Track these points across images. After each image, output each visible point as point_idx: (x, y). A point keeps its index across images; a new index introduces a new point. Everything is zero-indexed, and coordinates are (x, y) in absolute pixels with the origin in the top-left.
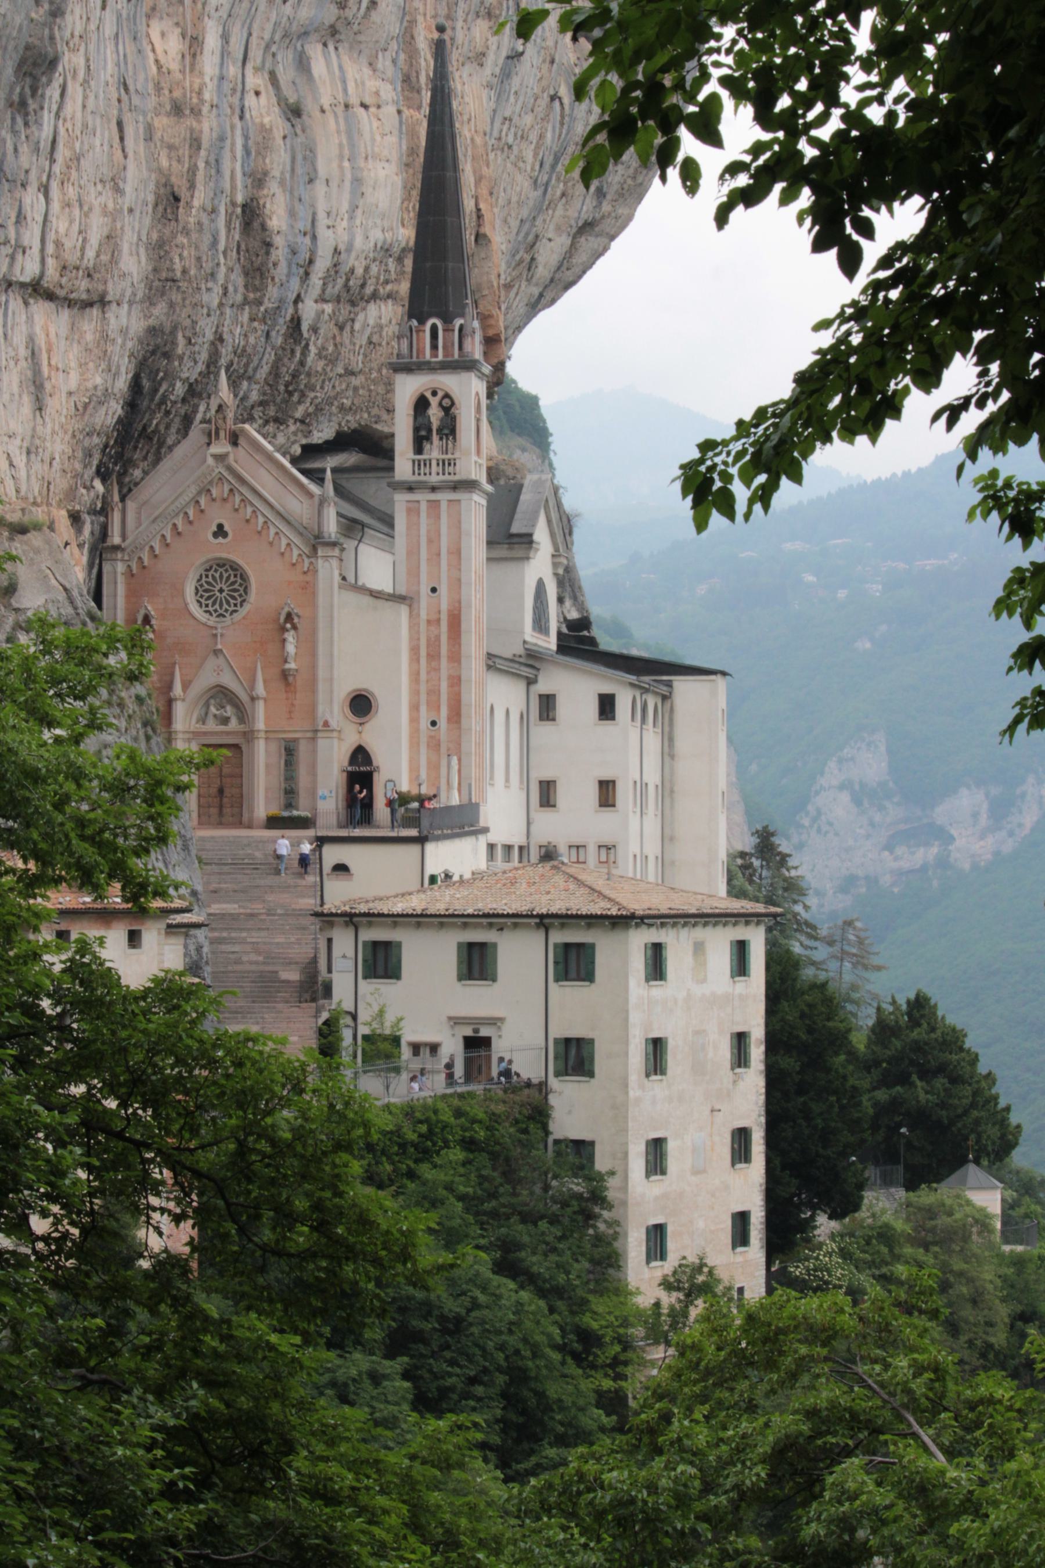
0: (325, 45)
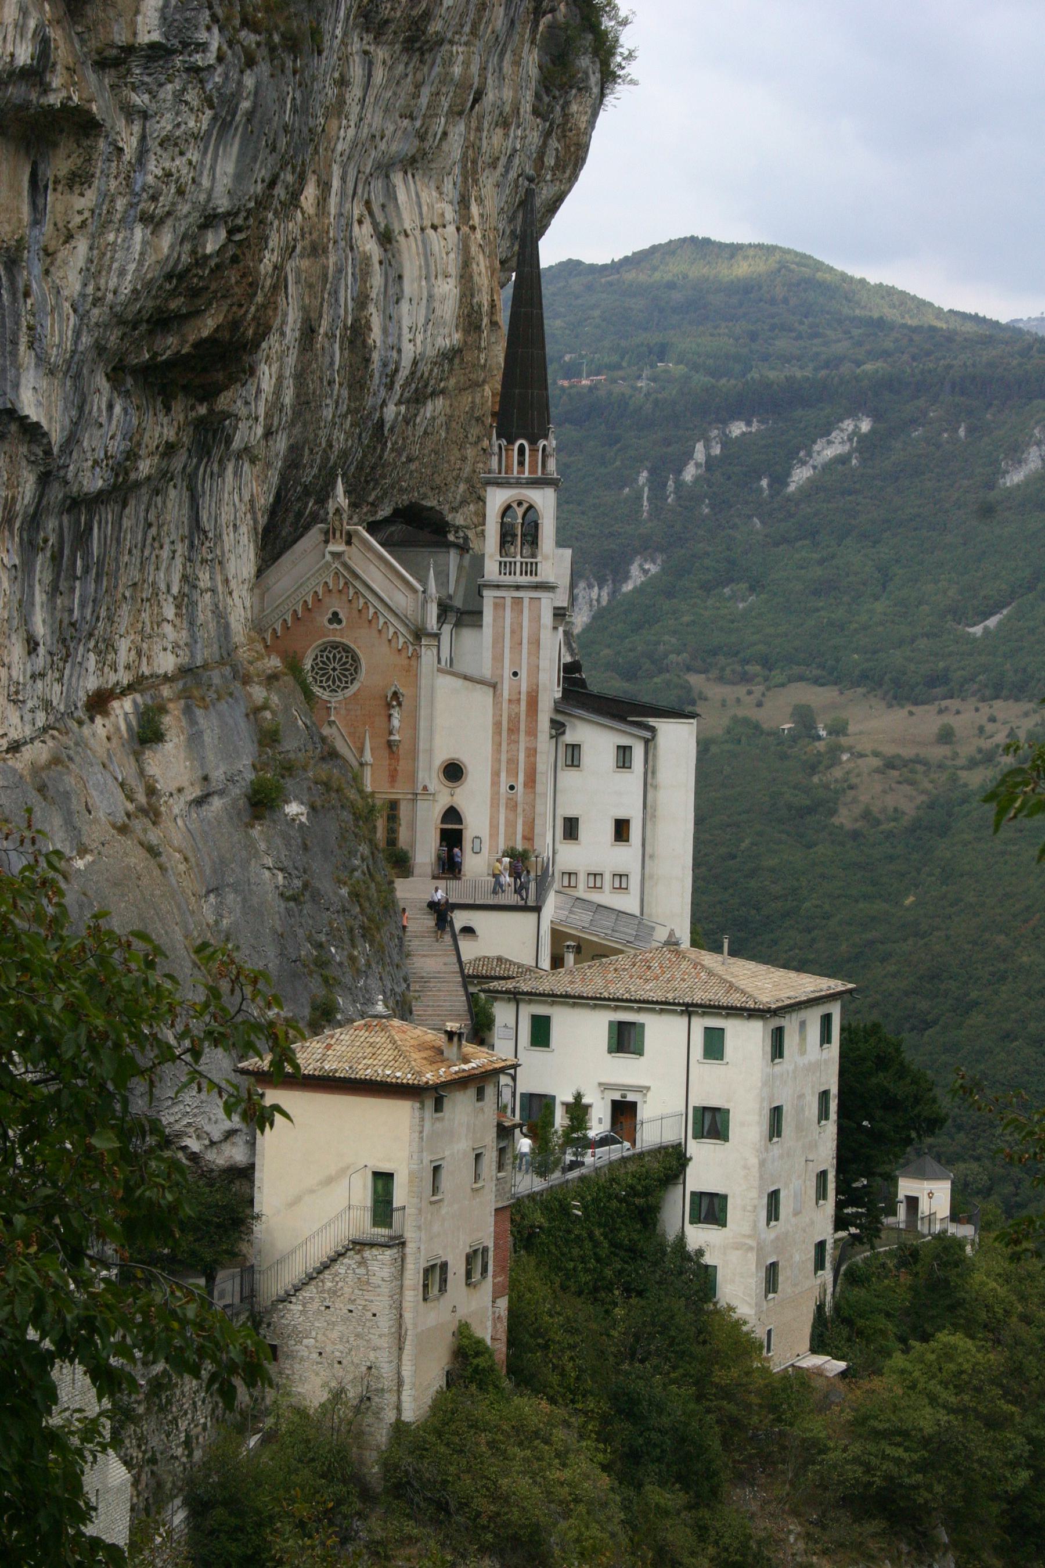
0: (406, 173)
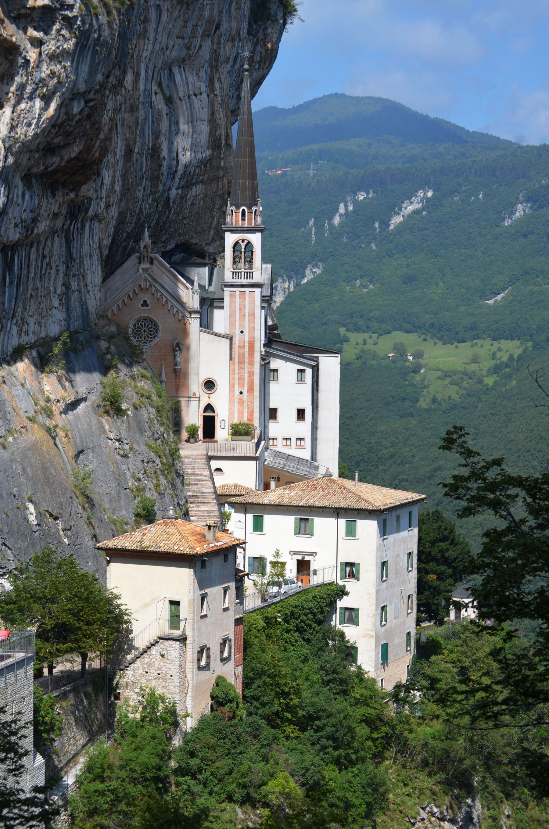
0: (180, 67)
